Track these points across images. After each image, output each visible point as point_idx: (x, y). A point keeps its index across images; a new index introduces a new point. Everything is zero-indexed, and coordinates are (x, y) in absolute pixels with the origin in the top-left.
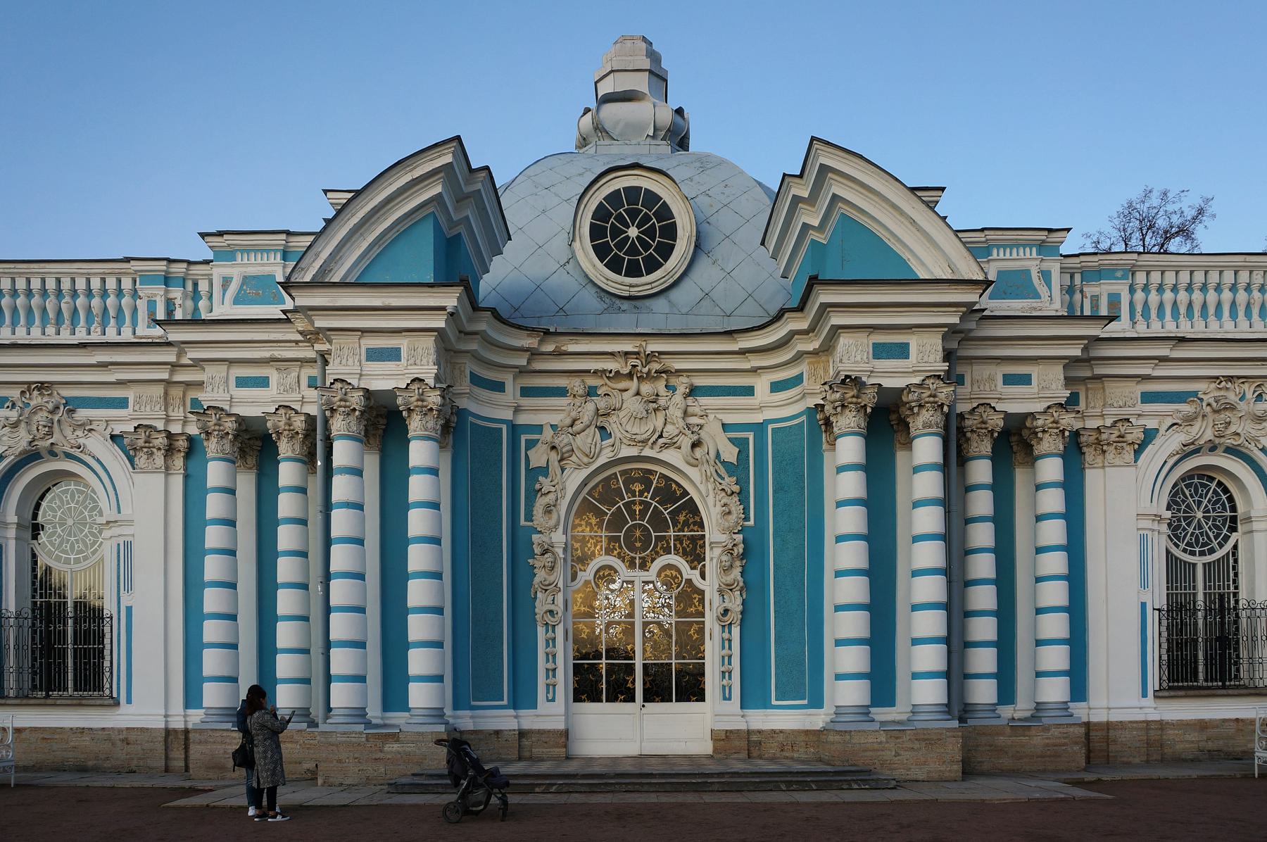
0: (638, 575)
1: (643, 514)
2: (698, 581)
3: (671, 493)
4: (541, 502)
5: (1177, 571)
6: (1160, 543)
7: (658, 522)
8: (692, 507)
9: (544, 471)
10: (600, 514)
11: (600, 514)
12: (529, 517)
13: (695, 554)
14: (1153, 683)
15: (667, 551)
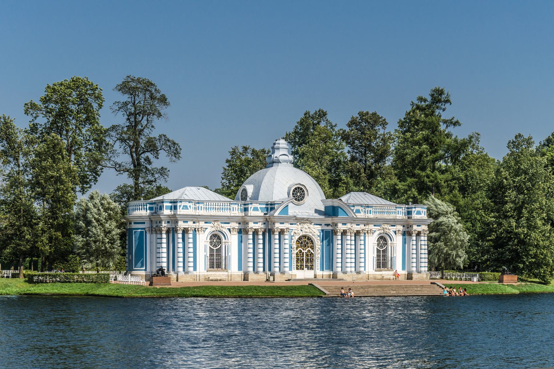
0: (304, 251)
1: (305, 242)
2: (313, 253)
3: (309, 239)
4: (293, 241)
5: (378, 251)
6: (376, 247)
7: (307, 243)
8: (312, 241)
9: (293, 236)
10: (298, 241)
11: (298, 241)
12: (291, 243)
13: (312, 248)
14: (375, 268)
15: (308, 247)
